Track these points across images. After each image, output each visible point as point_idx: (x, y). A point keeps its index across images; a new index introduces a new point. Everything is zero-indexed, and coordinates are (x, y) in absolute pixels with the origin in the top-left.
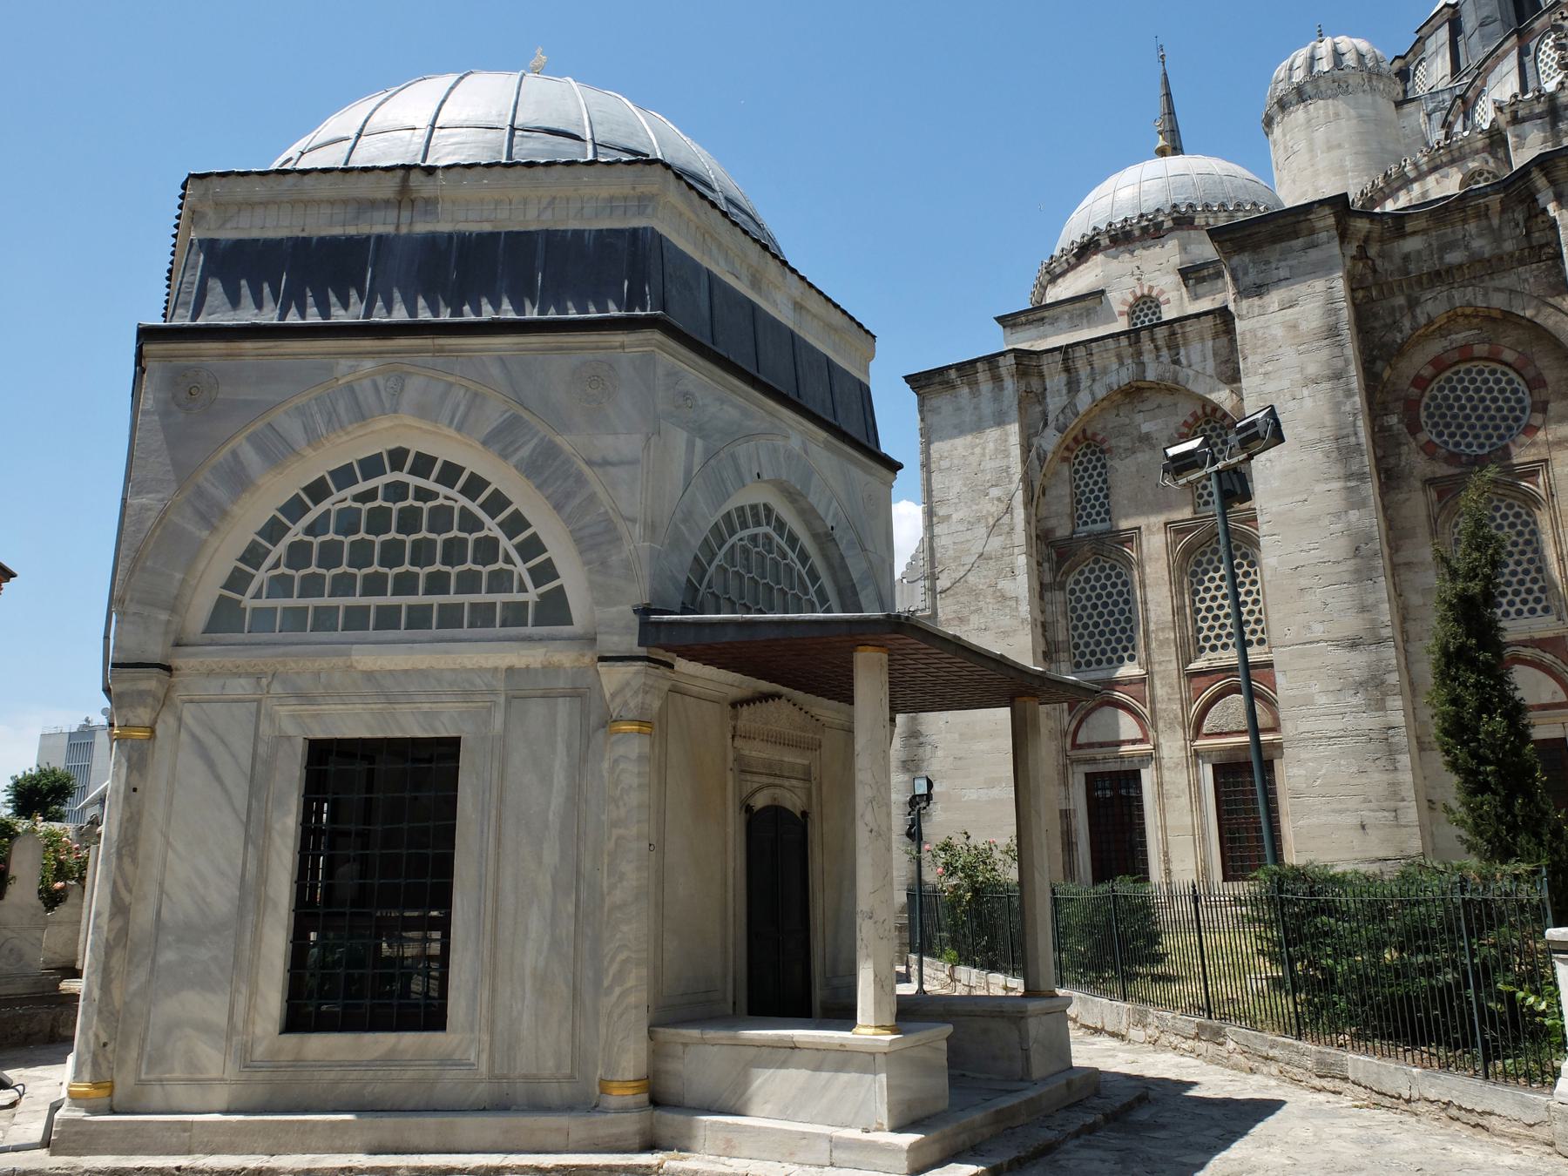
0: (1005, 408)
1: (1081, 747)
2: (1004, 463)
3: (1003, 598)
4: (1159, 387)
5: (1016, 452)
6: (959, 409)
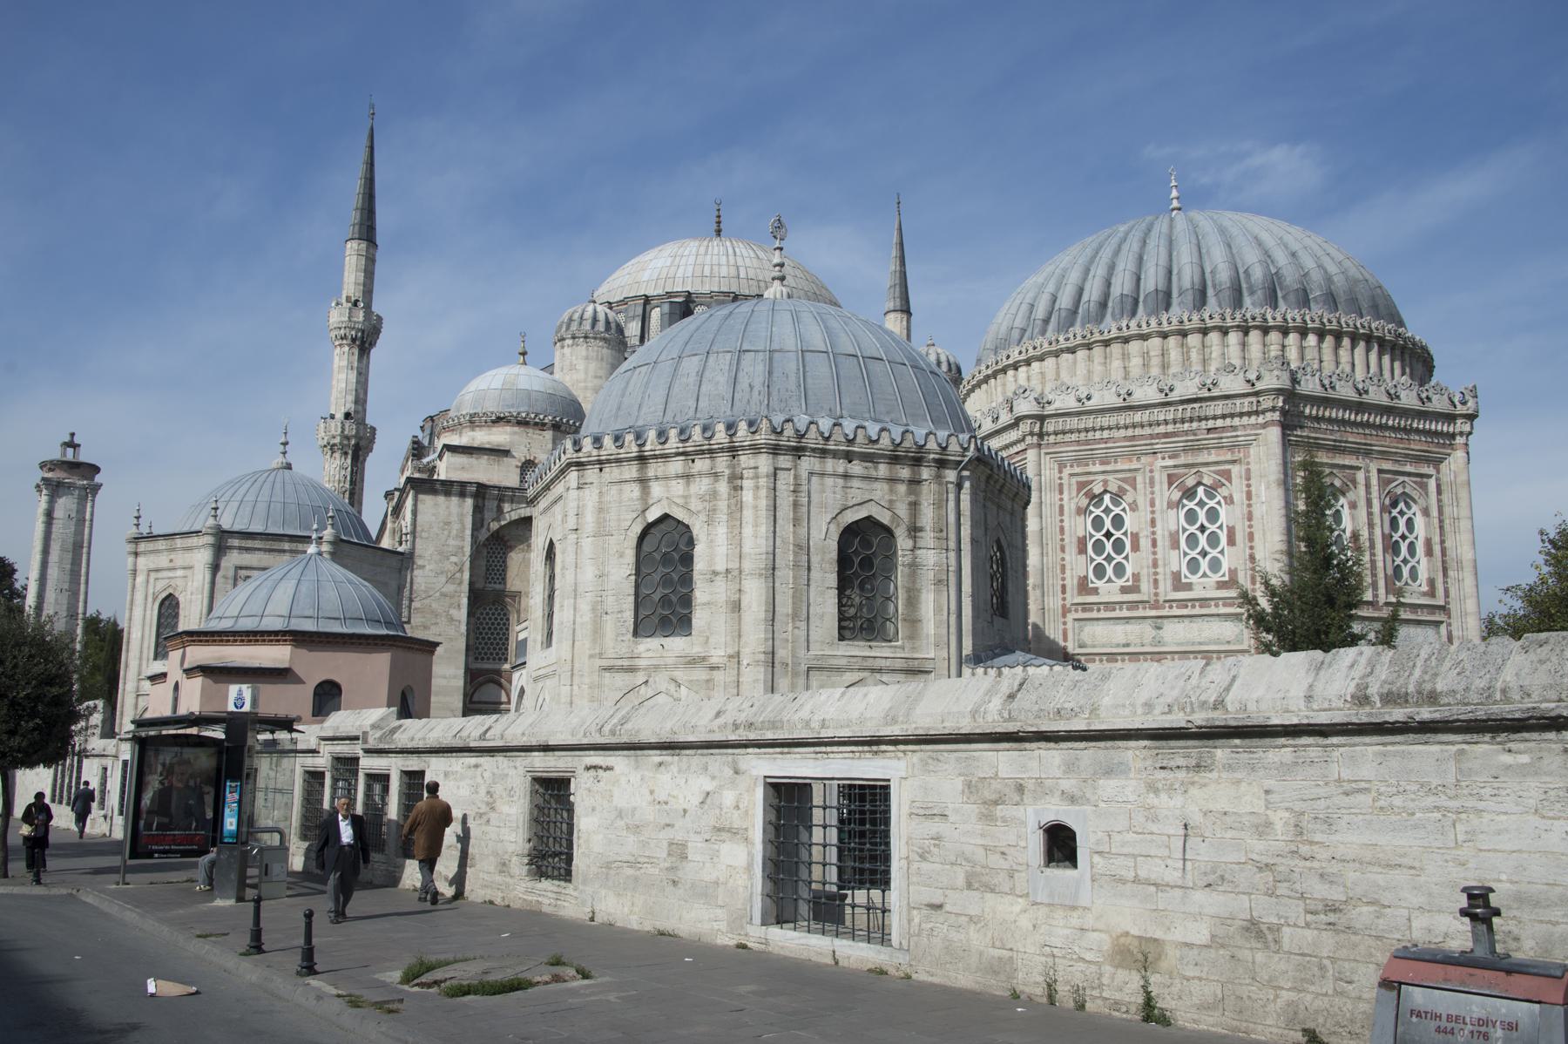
0: (465, 512)
1: (474, 703)
2: (460, 544)
3: (451, 619)
5: (468, 539)
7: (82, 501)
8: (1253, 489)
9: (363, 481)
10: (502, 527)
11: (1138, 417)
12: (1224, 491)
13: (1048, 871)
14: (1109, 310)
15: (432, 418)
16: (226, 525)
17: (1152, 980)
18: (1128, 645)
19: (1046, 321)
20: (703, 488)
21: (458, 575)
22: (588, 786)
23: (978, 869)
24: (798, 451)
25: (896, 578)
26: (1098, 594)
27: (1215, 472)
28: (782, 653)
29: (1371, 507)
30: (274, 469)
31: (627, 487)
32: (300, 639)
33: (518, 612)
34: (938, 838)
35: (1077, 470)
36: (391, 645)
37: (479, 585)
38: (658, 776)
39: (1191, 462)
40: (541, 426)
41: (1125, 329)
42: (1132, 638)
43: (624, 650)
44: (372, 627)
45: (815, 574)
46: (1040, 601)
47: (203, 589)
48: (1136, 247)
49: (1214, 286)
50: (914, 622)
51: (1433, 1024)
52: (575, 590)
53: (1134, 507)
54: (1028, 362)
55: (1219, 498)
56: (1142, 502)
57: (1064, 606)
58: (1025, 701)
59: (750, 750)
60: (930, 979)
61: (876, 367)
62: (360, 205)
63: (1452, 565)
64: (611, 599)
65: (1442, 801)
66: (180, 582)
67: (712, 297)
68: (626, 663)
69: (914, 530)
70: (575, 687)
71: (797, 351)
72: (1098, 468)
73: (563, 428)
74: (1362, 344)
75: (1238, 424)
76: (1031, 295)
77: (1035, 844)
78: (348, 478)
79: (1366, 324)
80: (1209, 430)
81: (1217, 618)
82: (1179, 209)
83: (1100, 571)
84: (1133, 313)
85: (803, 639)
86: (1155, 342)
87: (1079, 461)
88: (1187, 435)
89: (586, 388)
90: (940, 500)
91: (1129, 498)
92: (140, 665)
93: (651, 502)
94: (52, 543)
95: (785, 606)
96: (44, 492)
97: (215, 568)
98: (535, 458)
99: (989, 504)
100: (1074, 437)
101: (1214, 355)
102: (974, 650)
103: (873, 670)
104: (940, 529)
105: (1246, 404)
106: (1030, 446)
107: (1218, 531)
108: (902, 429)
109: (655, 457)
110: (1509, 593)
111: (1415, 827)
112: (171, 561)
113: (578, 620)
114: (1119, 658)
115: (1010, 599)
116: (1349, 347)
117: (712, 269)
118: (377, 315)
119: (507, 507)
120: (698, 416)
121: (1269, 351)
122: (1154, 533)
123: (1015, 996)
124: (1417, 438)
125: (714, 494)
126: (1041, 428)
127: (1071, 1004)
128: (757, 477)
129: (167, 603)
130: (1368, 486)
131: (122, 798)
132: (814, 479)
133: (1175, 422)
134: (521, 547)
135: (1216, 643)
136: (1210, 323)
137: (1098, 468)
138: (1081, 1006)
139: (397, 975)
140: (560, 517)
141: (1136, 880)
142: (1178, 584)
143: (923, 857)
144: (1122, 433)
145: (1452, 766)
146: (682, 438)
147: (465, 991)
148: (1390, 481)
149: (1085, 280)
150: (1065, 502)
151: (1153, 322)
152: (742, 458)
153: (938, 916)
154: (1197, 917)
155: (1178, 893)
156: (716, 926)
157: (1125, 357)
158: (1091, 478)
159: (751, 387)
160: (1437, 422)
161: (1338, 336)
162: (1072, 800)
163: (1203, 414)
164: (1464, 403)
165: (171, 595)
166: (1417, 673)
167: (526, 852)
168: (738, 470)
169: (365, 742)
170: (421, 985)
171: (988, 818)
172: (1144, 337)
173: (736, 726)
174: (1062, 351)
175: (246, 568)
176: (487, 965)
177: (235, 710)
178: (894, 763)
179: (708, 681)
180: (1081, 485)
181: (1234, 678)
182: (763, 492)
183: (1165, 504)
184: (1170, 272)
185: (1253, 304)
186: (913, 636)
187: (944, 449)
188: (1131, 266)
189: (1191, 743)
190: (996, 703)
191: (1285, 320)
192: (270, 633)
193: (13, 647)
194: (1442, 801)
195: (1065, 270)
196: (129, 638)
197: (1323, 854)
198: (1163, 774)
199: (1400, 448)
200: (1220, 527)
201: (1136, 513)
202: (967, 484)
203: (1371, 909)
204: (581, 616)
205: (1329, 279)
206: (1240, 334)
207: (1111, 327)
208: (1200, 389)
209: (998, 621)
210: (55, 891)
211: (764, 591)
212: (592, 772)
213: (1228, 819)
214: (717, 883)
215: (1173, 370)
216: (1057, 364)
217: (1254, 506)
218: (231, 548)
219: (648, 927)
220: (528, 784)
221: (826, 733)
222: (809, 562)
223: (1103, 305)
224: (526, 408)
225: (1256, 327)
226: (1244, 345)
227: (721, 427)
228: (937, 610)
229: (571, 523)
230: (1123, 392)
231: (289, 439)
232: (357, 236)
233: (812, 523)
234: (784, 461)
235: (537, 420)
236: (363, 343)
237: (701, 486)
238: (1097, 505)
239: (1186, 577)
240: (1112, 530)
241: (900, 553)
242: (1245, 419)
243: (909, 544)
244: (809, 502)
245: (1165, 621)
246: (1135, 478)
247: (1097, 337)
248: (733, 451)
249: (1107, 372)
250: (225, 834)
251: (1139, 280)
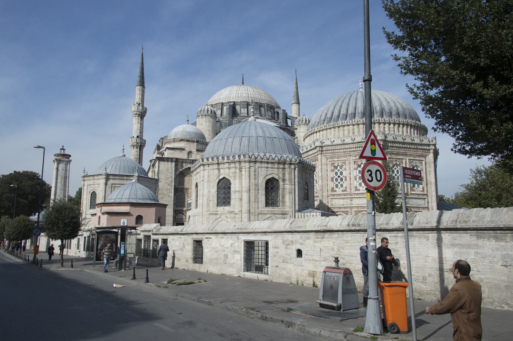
1: (176, 219)
2: (172, 175)
3: (169, 196)
5: (174, 174)
7: (66, 165)
9: (142, 155)
10: (183, 170)
11: (346, 146)
13: (297, 259)
14: (340, 118)
16: (109, 172)
17: (315, 279)
18: (344, 205)
19: (324, 120)
23: (285, 258)
24: (255, 162)
26: (336, 192)
28: (252, 210)
30: (121, 157)
31: (215, 170)
32: (132, 204)
33: (188, 194)
35: (331, 160)
37: (177, 186)
40: (193, 141)
46: (321, 194)
48: (347, 101)
50: (284, 202)
51: (329, 277)
52: (203, 195)
53: (345, 169)
54: (319, 131)
56: (347, 168)
57: (328, 195)
58: (293, 224)
59: (241, 234)
60: (276, 281)
61: (275, 140)
62: (140, 76)
63: (429, 183)
64: (211, 197)
66: (96, 188)
68: (215, 213)
69: (284, 180)
70: (203, 219)
72: (336, 159)
73: (199, 142)
74: (405, 126)
76: (320, 113)
77: (295, 253)
79: (407, 121)
82: (362, 88)
83: (337, 186)
84: (346, 119)
85: (257, 206)
86: (351, 127)
87: (331, 158)
90: (290, 173)
91: (344, 167)
94: (58, 177)
95: (252, 199)
96: (56, 162)
97: (106, 184)
99: (303, 173)
100: (330, 151)
103: (274, 214)
104: (290, 180)
106: (319, 154)
108: (281, 156)
109: (221, 163)
110: (462, 187)
111: (356, 249)
112: (94, 182)
113: (204, 202)
115: (309, 195)
116: (402, 127)
118: (146, 108)
119: (184, 165)
120: (232, 153)
122: (350, 176)
123: (291, 284)
124: (420, 150)
125: (235, 172)
126: (322, 149)
127: (301, 285)
129: (93, 194)
131: (84, 246)
132: (259, 169)
137: (336, 159)
138: (303, 285)
139: (166, 282)
140: (199, 177)
141: (312, 260)
142: (356, 189)
143: (275, 256)
144: (342, 150)
146: (228, 159)
147: (181, 284)
148: (412, 162)
150: (328, 168)
151: (351, 122)
152: (242, 164)
153: (277, 268)
156: (234, 272)
157: (344, 130)
158: (334, 162)
159: (244, 146)
160: (425, 146)
161: (399, 124)
162: (301, 244)
164: (432, 141)
165: (94, 191)
166: (358, 220)
167: (192, 257)
168: (241, 167)
169: (152, 232)
170: (172, 284)
171: (286, 248)
172: (348, 125)
173: (238, 229)
174: (328, 129)
176: (185, 280)
179: (234, 217)
180: (332, 164)
181: (329, 221)
182: (247, 172)
184: (356, 108)
185: (377, 116)
186: (283, 206)
187: (291, 160)
191: (385, 121)
192: (124, 203)
193: (64, 210)
196: (83, 203)
197: (342, 254)
198: (317, 239)
199: (415, 153)
201: (346, 171)
202: (297, 169)
203: (350, 264)
205: (398, 109)
207: (340, 123)
209: (306, 201)
210: (77, 269)
211: (247, 195)
212: (207, 239)
213: (327, 248)
214: (234, 263)
215: (356, 134)
216: (327, 132)
218: (110, 179)
219: (220, 273)
221: (256, 231)
222: (258, 188)
223: (338, 117)
225: (377, 123)
227: (237, 156)
228: (289, 199)
229: (202, 179)
230: (342, 140)
231: (124, 148)
234: (252, 164)
236: (142, 116)
237: (232, 170)
238: (336, 169)
240: (340, 176)
243: (283, 183)
244: (258, 174)
245: (353, 199)
246: (346, 162)
247: (336, 125)
248: (240, 162)
249: (339, 134)
250: (121, 254)
251: (348, 110)
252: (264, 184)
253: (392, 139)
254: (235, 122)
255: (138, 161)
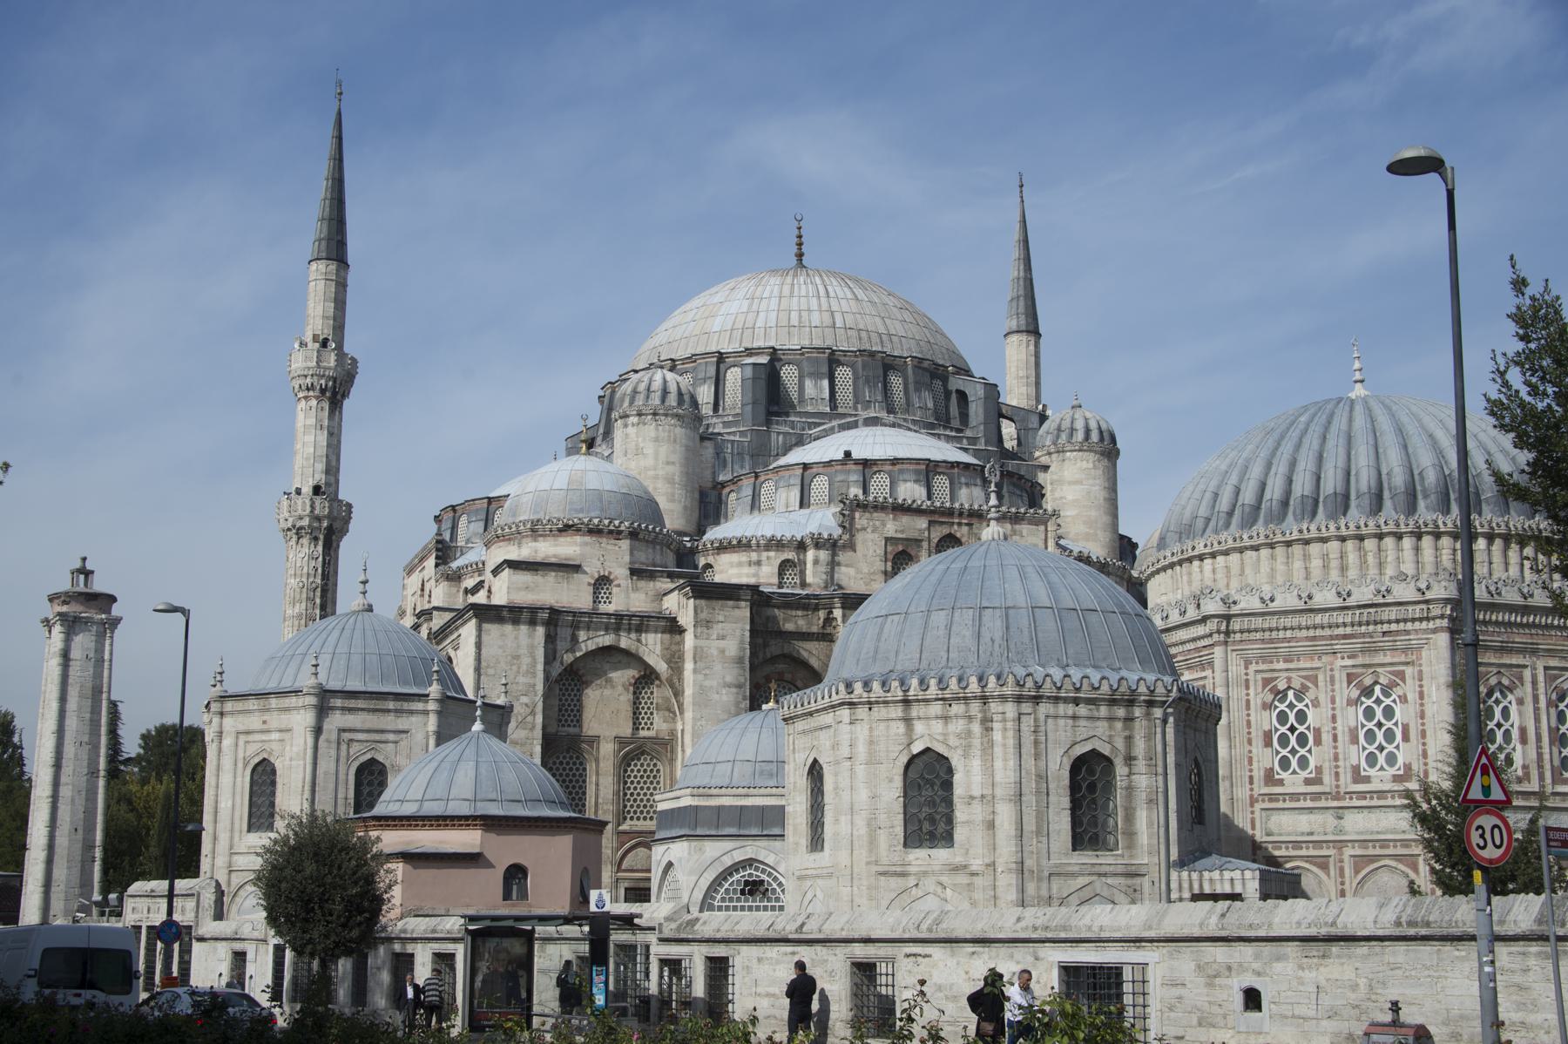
0: (536, 643)
2: (532, 681)
4: (626, 653)
5: (540, 675)
6: (502, 635)
7: (101, 638)
8: (1425, 689)
9: (337, 573)
10: (577, 659)
11: (1318, 619)
12: (1398, 691)
14: (1291, 509)
15: (453, 508)
18: (1312, 834)
19: (1230, 514)
20: (960, 728)
21: (530, 719)
22: (909, 968)
23: (1205, 1015)
24: (1036, 699)
25: (1116, 797)
26: (1284, 785)
27: (1390, 672)
28: (1029, 863)
29: (1538, 703)
30: (354, 612)
31: (893, 724)
32: (491, 823)
33: (597, 760)
34: (1180, 998)
35: (1262, 667)
36: (572, 827)
37: (552, 730)
38: (972, 961)
39: (1367, 662)
40: (616, 534)
41: (1305, 531)
42: (1315, 828)
43: (896, 859)
44: (551, 809)
45: (1052, 798)
47: (305, 754)
49: (1390, 489)
50: (1131, 834)
52: (852, 809)
53: (1316, 703)
54: (1213, 555)
55: (1394, 696)
56: (1322, 698)
59: (1047, 945)
61: (1092, 617)
62: (327, 213)
64: (883, 816)
65: (1432, 973)
66: (275, 746)
67: (802, 354)
68: (899, 869)
69: (1130, 759)
70: (855, 888)
71: (1027, 608)
72: (1282, 665)
73: (641, 536)
75: (1411, 628)
77: (1239, 999)
78: (320, 571)
79: (1534, 526)
80: (1384, 633)
81: (1393, 809)
82: (1362, 381)
84: (1314, 514)
85: (1045, 851)
87: (1264, 659)
88: (1364, 637)
89: (656, 477)
91: (1311, 694)
92: (232, 838)
93: (915, 737)
94: (70, 688)
97: (318, 731)
98: (610, 573)
100: (1259, 635)
101: (1389, 559)
102: (1179, 856)
103: (1100, 875)
104: (1150, 758)
105: (1418, 611)
107: (1394, 727)
109: (918, 701)
112: (264, 722)
113: (855, 832)
114: (1304, 845)
115: (1206, 807)
117: (800, 317)
118: (353, 359)
119: (582, 635)
120: (950, 664)
121: (1441, 555)
122: (1334, 728)
125: (969, 733)
126: (1227, 626)
128: (1004, 720)
129: (260, 769)
130: (1534, 683)
133: (1353, 625)
134: (598, 682)
135: (1392, 833)
136: (1385, 529)
137: (1282, 665)
141: (1293, 1016)
143: (1171, 1009)
144: (1304, 633)
145: (1435, 956)
148: (1556, 677)
149: (1267, 474)
150: (1252, 697)
151: (1332, 527)
152: (992, 704)
154: (1324, 1033)
155: (1314, 1021)
157: (1306, 557)
158: (1276, 675)
161: (1507, 539)
162: (1259, 974)
163: (1378, 619)
165: (264, 759)
166: (1423, 911)
167: (850, 1018)
169: (660, 932)
171: (1210, 985)
172: (1324, 540)
174: (1246, 548)
175: (350, 730)
177: (597, 910)
178: (1151, 953)
179: (968, 884)
180: (1266, 682)
181: (1342, 910)
182: (1010, 734)
183: (1345, 701)
184: (1348, 474)
185: (1427, 508)
186: (1131, 846)
187: (1153, 691)
188: (1311, 466)
189: (1320, 944)
190: (1214, 920)
192: (460, 818)
194: (1432, 973)
195: (1248, 461)
198: (1306, 960)
200: (1396, 724)
202: (1171, 719)
204: (857, 830)
206: (1414, 539)
207: (1292, 528)
208: (1375, 596)
209: (1197, 828)
212: (912, 959)
213: (1339, 983)
215: (1353, 573)
216: (1242, 560)
217: (1426, 706)
220: (848, 968)
221: (1104, 935)
222: (1047, 789)
223: (1285, 503)
224: (597, 513)
226: (1417, 549)
227: (974, 680)
228: (1150, 824)
229: (845, 752)
230: (1304, 595)
231: (368, 577)
232: (324, 255)
233: (1049, 757)
234: (1026, 707)
235: (612, 528)
236: (334, 394)
237: (958, 726)
238: (1282, 701)
239: (1365, 770)
241: (1118, 778)
242: (1417, 623)
244: (1046, 740)
245: (1346, 811)
246: (1316, 677)
247: (1279, 538)
249: (1289, 573)
251: (1318, 479)
252: (1066, 774)
253: (1485, 595)
254: (781, 438)
255: (318, 601)
